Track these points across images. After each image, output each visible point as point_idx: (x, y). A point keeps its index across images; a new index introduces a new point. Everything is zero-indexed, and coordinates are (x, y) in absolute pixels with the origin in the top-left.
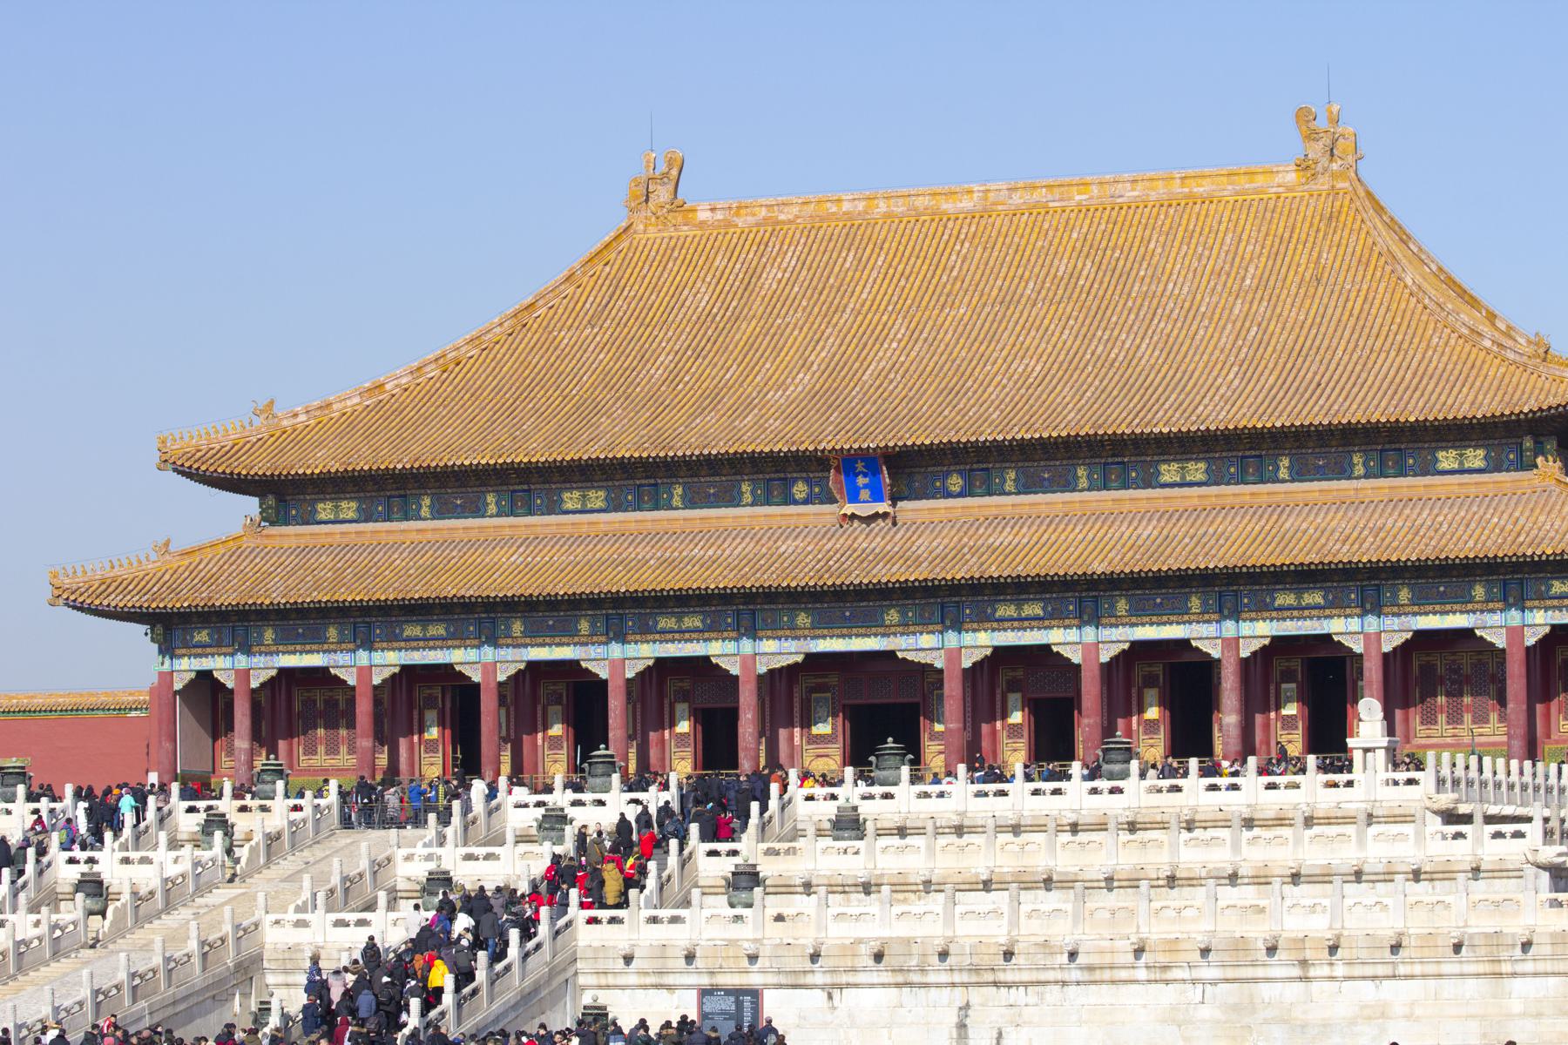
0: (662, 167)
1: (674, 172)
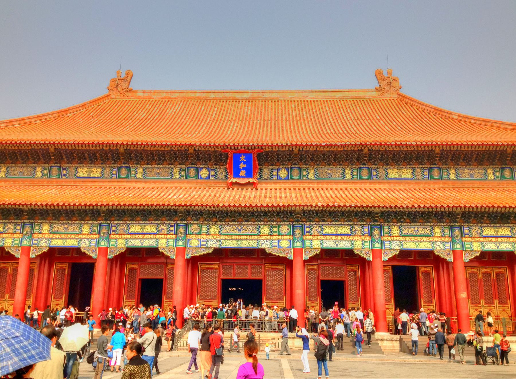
0: (123, 76)
1: (129, 78)
